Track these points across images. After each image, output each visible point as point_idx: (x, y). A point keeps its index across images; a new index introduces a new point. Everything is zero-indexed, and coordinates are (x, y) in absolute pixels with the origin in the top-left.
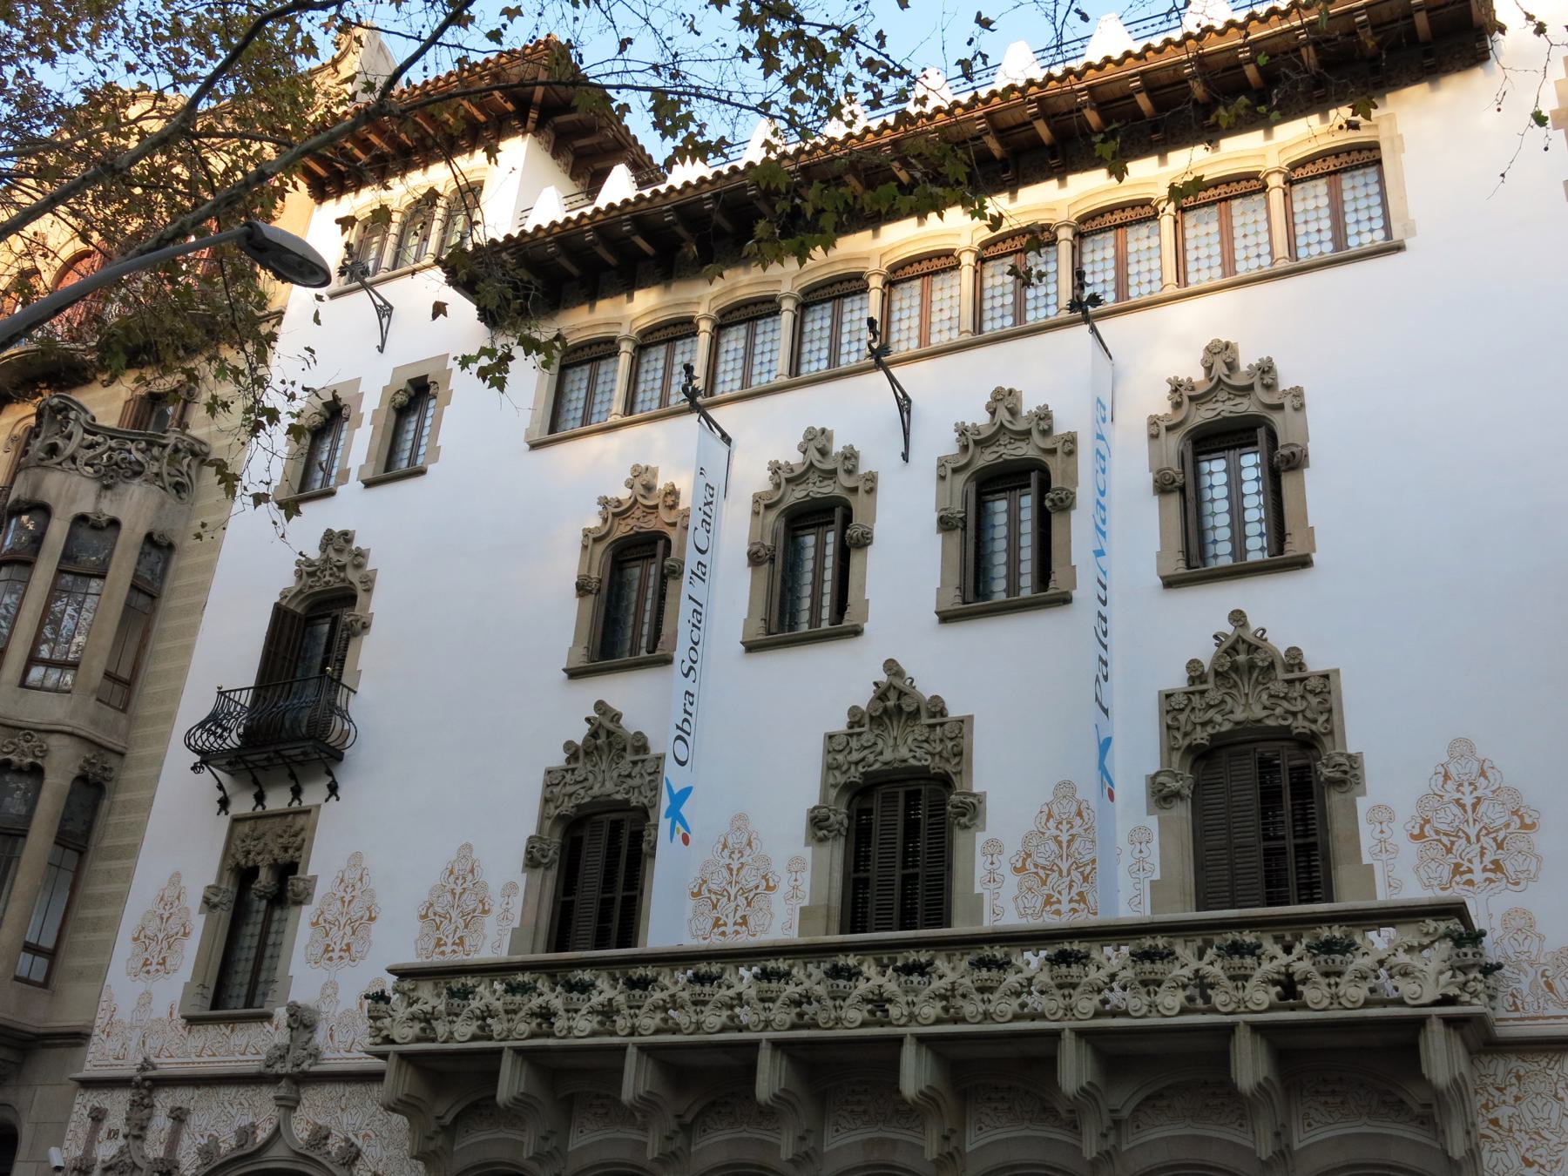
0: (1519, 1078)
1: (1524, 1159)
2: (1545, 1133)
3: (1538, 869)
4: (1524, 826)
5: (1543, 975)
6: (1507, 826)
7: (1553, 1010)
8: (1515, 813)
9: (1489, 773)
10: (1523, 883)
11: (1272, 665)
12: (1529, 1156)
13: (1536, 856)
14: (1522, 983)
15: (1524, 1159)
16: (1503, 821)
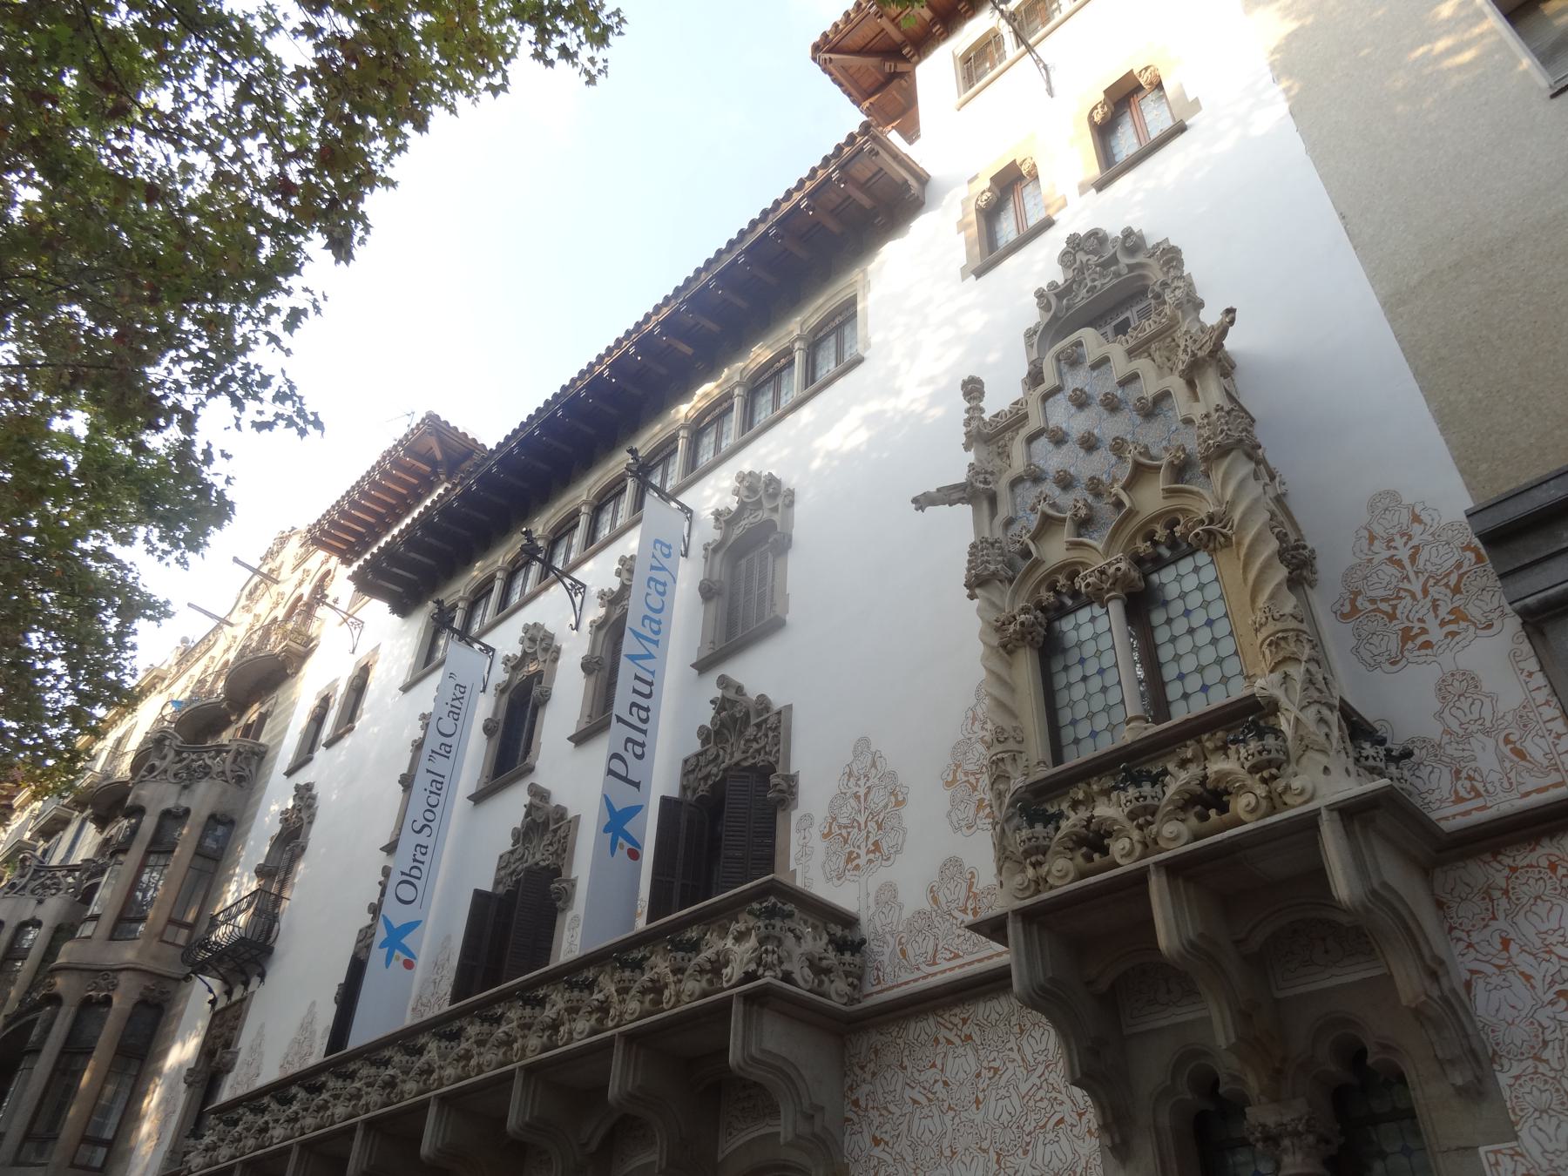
0: (876, 1052)
1: (874, 1138)
2: (891, 1107)
7: (905, 977)
11: (747, 714)
12: (877, 1134)
14: (883, 953)
15: (874, 1138)
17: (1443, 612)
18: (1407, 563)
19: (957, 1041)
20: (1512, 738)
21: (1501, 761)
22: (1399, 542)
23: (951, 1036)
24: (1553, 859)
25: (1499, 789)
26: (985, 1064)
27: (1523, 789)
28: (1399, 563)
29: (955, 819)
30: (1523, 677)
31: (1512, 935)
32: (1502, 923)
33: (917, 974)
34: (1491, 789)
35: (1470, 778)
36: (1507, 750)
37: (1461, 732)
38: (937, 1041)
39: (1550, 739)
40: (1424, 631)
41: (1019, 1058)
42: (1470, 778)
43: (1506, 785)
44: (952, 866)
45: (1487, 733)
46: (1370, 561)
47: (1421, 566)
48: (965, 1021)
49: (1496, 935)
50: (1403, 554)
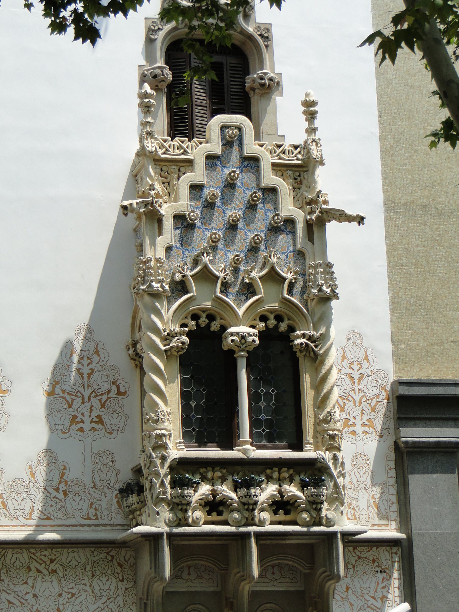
41: (89, 590)
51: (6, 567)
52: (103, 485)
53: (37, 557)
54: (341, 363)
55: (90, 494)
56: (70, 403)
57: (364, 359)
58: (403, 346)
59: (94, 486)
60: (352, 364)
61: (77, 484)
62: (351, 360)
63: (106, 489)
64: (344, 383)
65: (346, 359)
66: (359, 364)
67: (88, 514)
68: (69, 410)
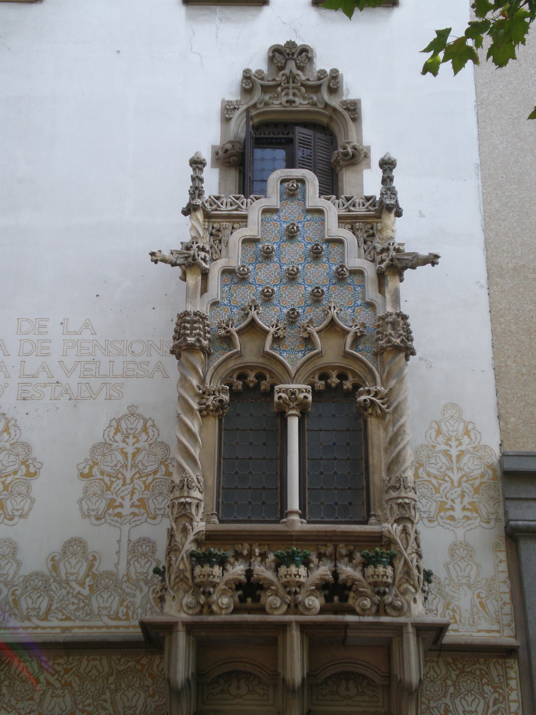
3: (30, 509)
4: (29, 474)
5: (13, 594)
6: (15, 472)
8: (23, 463)
9: (12, 431)
10: (16, 519)
13: (31, 498)
16: (13, 468)
17: (467, 500)
18: (454, 459)
19: (58, 685)
20: (482, 595)
21: (473, 606)
22: (454, 443)
23: (52, 680)
24: (483, 672)
25: (467, 623)
26: (80, 707)
27: (479, 627)
28: (450, 457)
29: (85, 507)
30: (497, 561)
31: (451, 708)
32: (447, 701)
33: (27, 624)
34: (463, 621)
35: (453, 610)
36: (477, 601)
37: (456, 581)
38: (38, 682)
39: (500, 604)
40: (452, 509)
42: (453, 610)
43: (471, 622)
44: (75, 546)
45: (469, 587)
46: (434, 447)
47: (462, 465)
48: (67, 671)
49: (443, 706)
50: (454, 452)
51: (10, 679)
52: (138, 578)
53: (49, 666)
54: (436, 439)
55: (121, 589)
56: (109, 485)
57: (465, 434)
58: (513, 419)
59: (128, 580)
60: (450, 439)
61: (107, 577)
62: (447, 435)
63: (142, 583)
64: (438, 461)
65: (441, 434)
66: (457, 440)
67: (117, 613)
68: (106, 493)
